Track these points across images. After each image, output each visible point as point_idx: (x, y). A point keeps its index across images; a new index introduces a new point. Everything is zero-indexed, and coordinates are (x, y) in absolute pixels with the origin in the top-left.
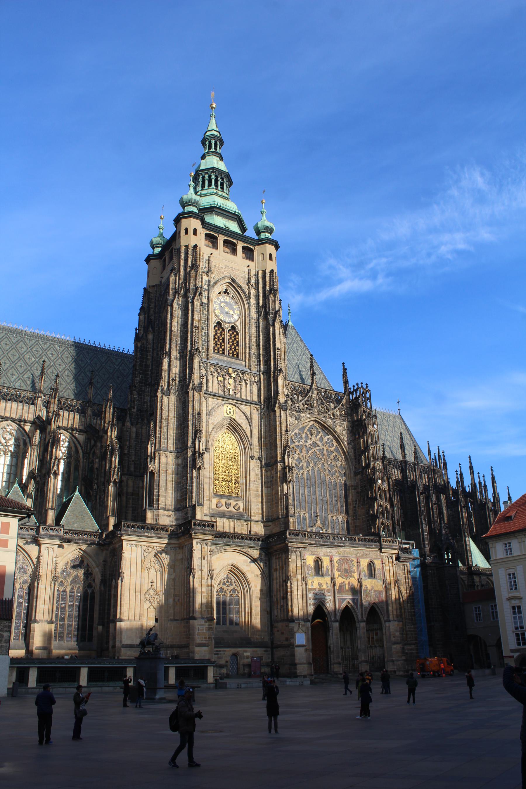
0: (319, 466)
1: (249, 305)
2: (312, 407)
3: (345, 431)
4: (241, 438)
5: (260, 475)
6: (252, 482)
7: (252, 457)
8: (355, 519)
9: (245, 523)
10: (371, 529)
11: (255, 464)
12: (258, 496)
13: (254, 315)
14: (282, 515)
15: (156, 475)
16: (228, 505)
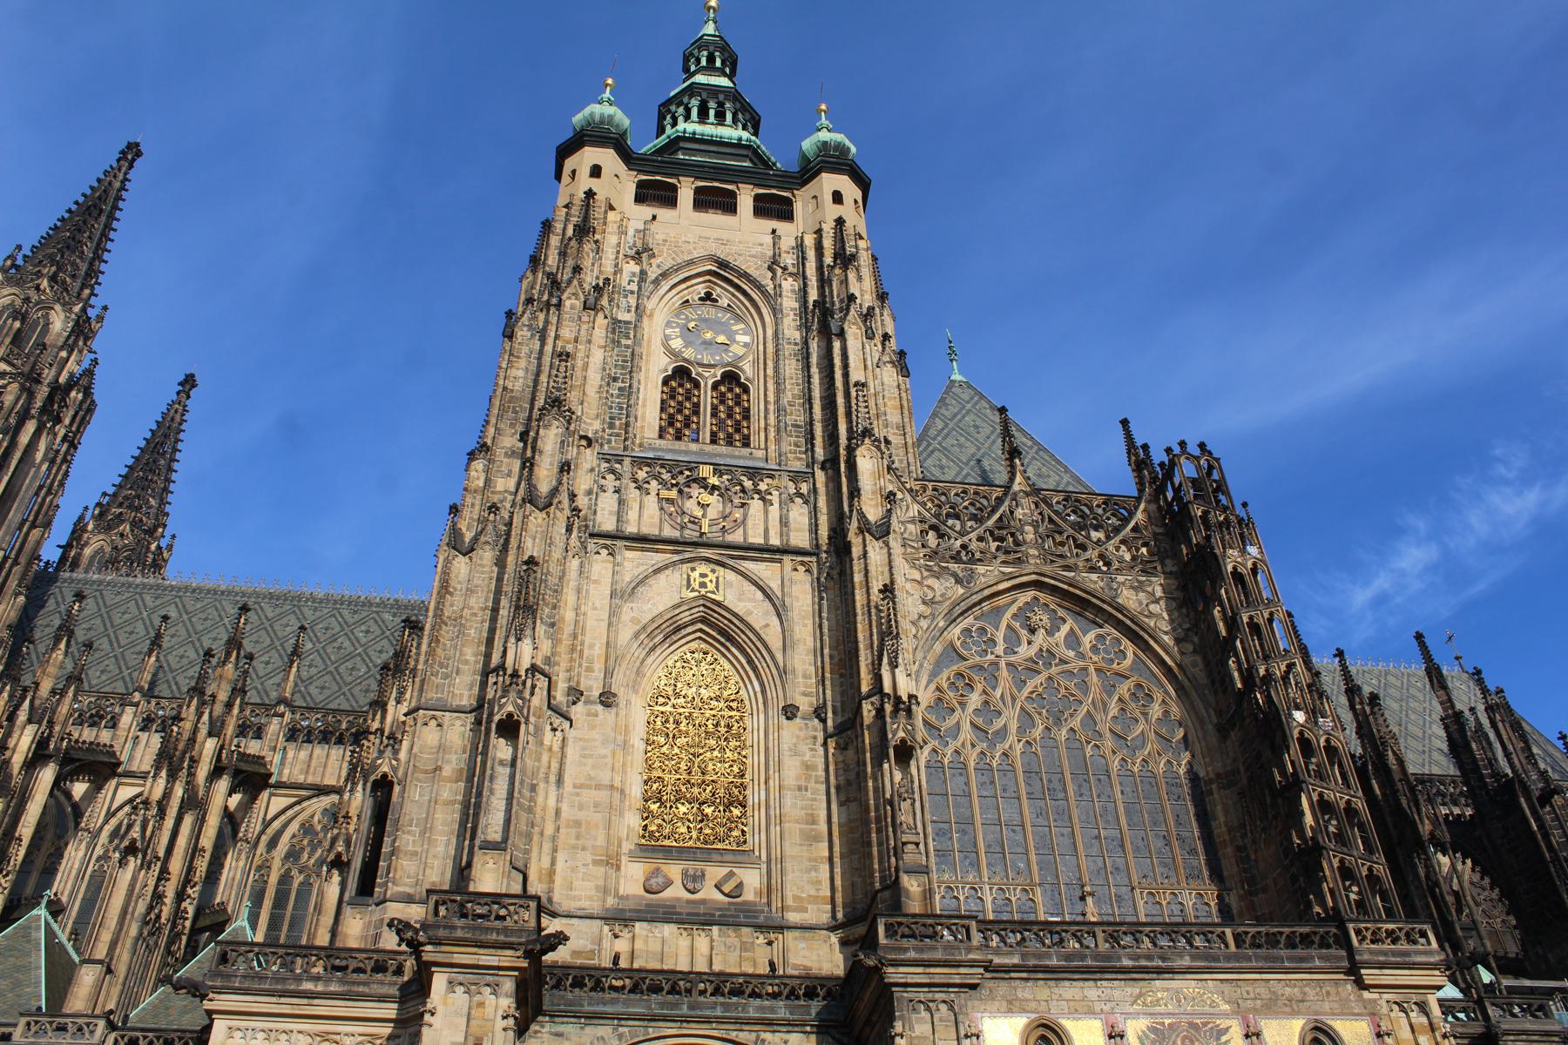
0: (1076, 723)
1: (776, 312)
2: (1017, 543)
3: (1157, 601)
4: (750, 661)
5: (821, 766)
6: (788, 794)
7: (790, 712)
8: (1251, 893)
9: (762, 940)
10: (1309, 906)
11: (802, 734)
12: (816, 838)
13: (791, 330)
14: (883, 879)
15: (397, 789)
16: (693, 881)
